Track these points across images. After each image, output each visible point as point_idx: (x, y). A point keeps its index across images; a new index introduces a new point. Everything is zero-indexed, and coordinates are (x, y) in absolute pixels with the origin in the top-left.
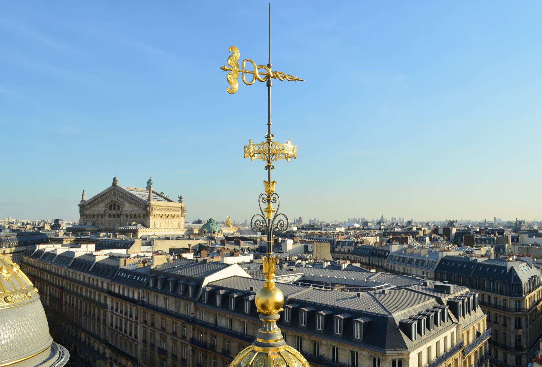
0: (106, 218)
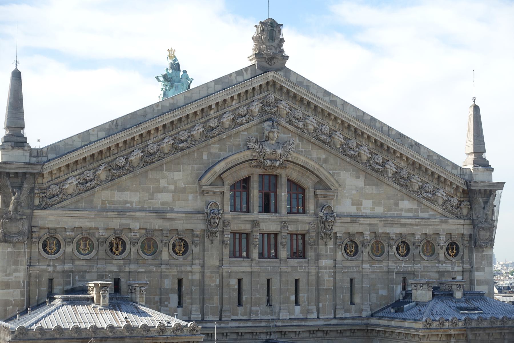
0: (212, 259)
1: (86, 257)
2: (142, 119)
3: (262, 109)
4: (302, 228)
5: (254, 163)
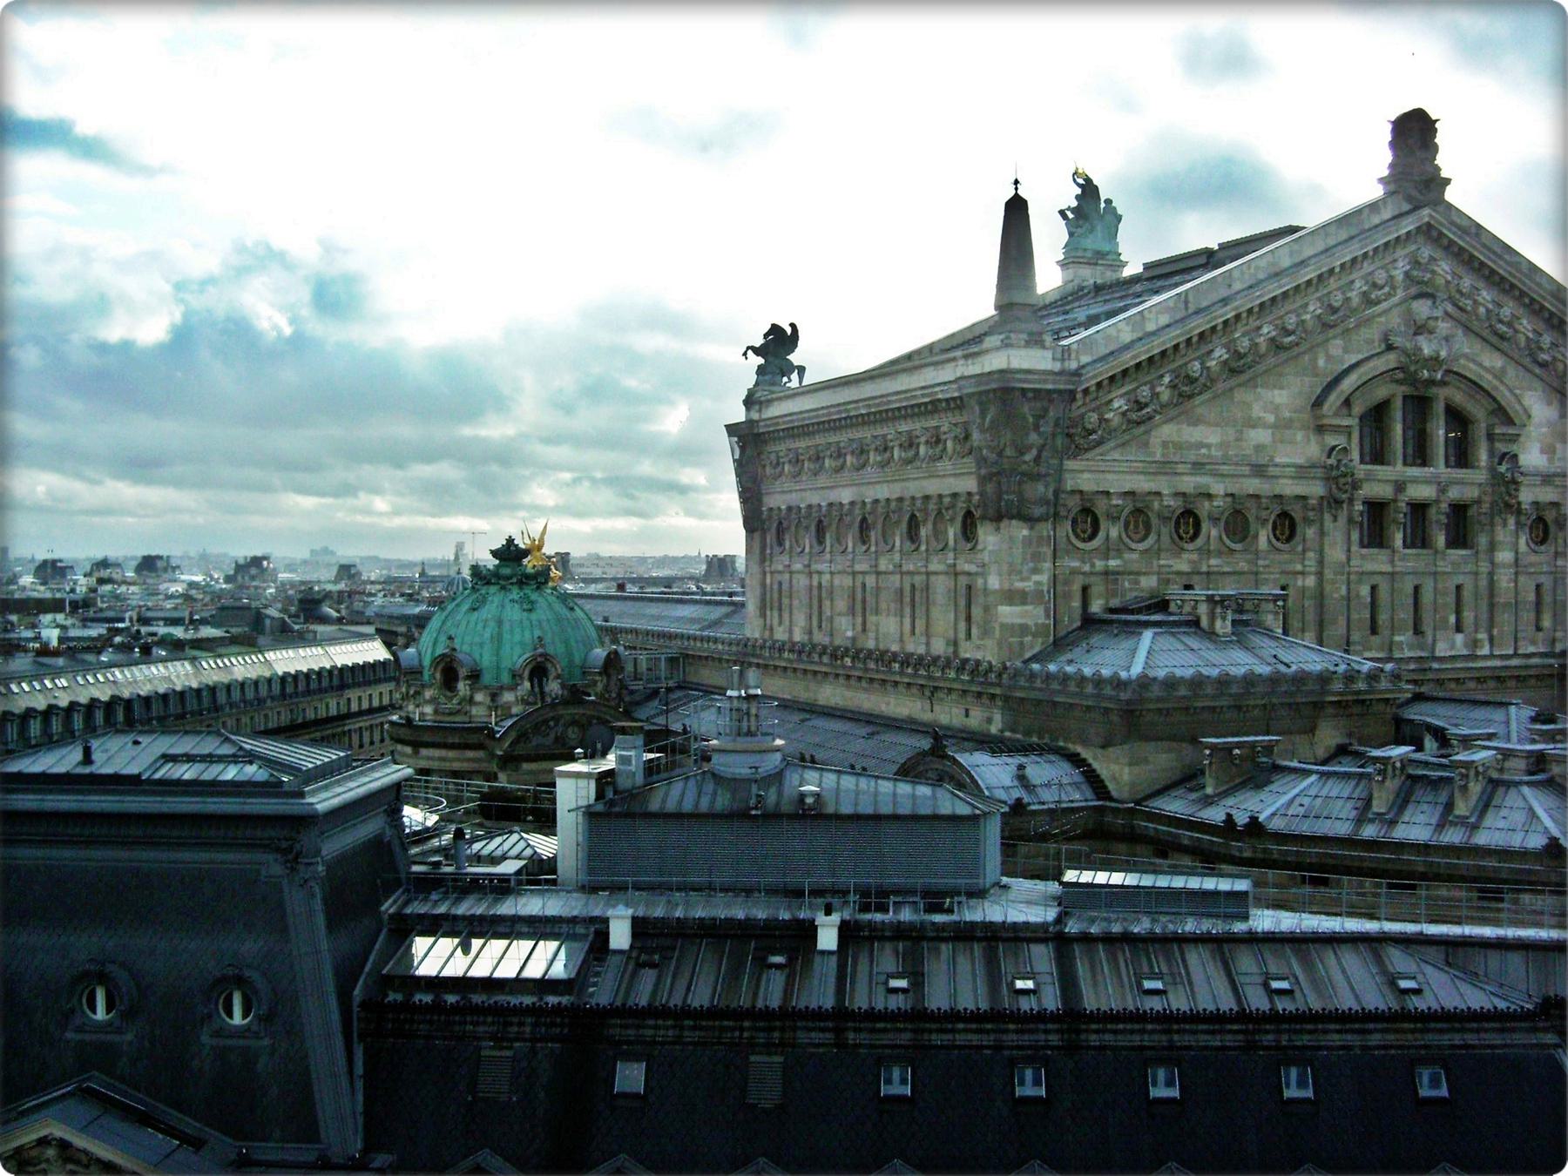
0: (1336, 554)
1: (1141, 546)
2: (1223, 293)
3: (1407, 274)
4: (1472, 493)
5: (1401, 376)
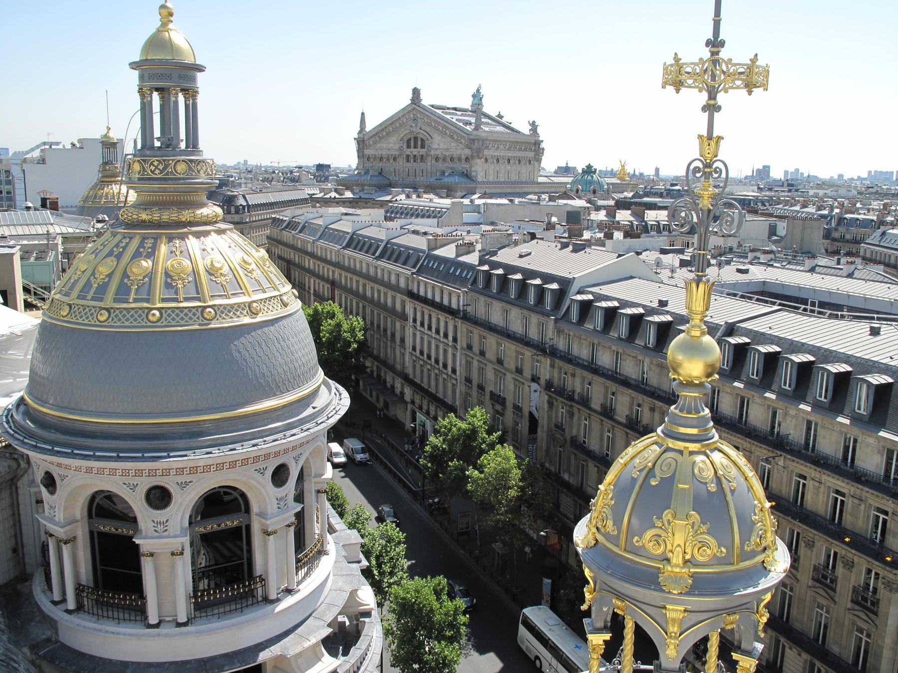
0: (401, 163)
